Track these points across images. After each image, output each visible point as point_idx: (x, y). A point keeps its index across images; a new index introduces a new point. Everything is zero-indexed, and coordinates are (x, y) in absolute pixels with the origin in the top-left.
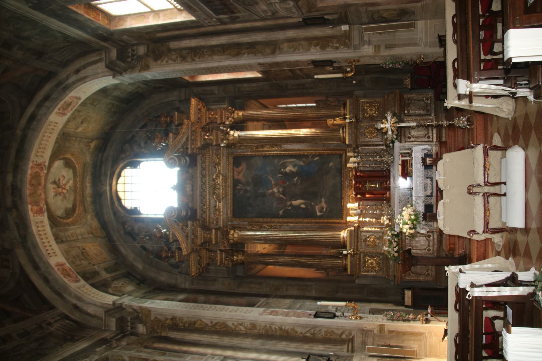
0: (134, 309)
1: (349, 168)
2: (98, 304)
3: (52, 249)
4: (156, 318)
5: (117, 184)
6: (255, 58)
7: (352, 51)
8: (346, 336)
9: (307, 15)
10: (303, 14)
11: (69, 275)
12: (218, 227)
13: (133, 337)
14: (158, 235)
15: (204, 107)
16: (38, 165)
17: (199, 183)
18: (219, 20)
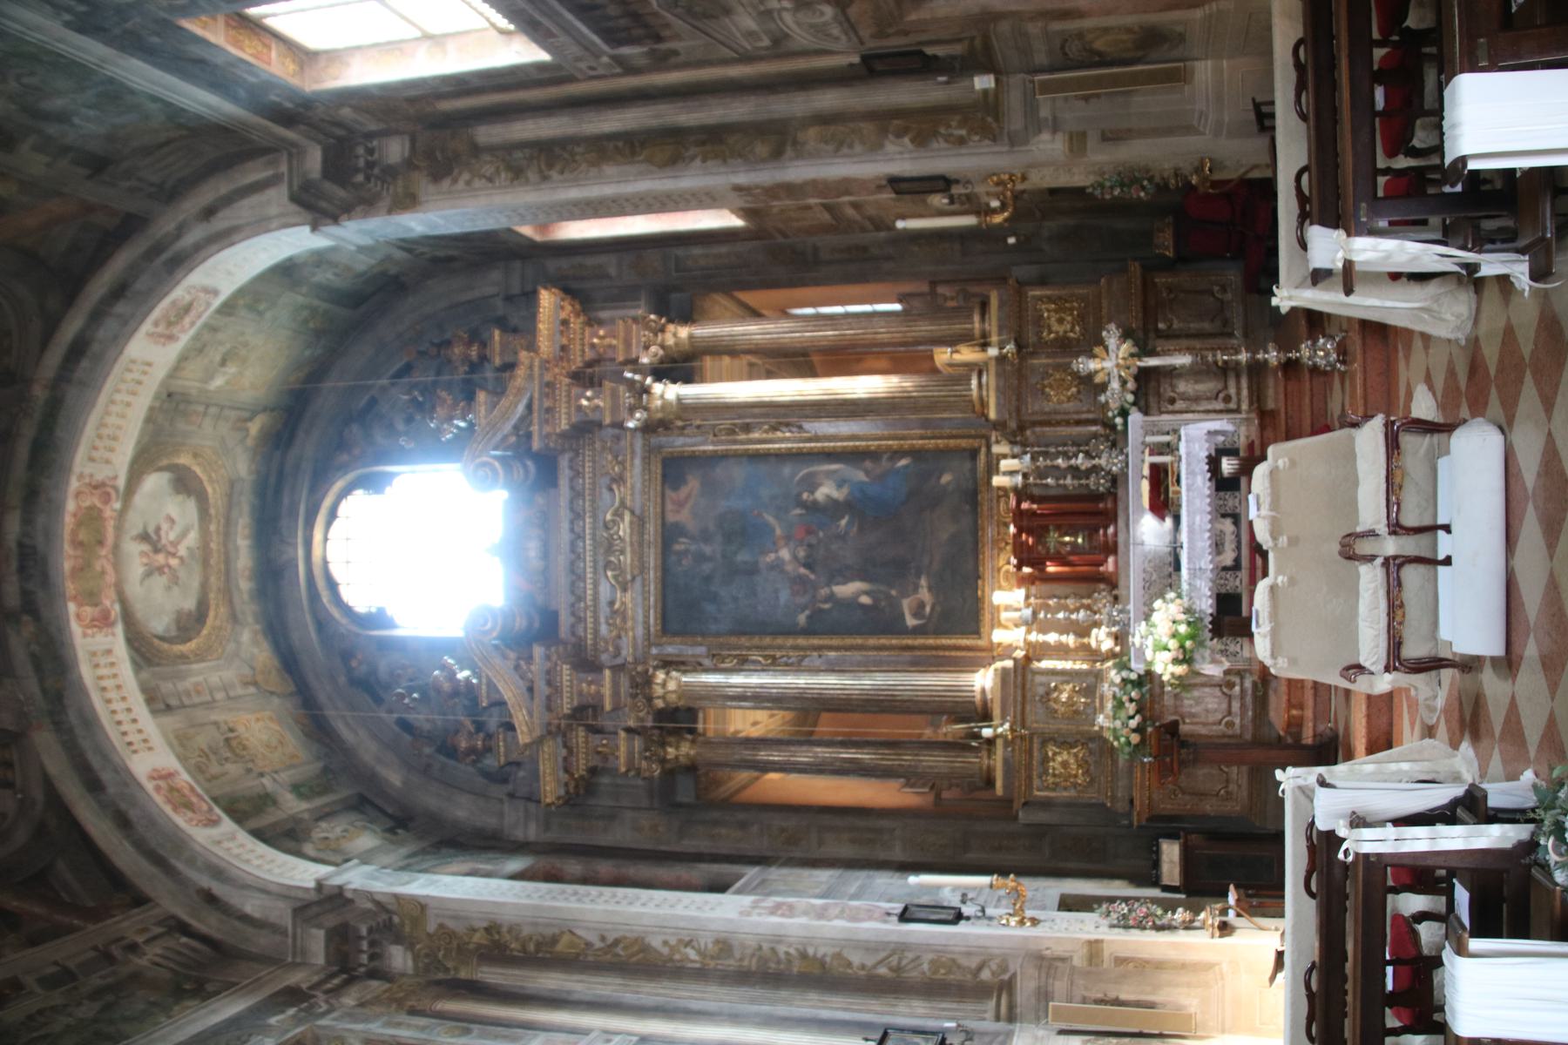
0: (378, 903)
1: (999, 488)
2: (272, 888)
3: (140, 731)
4: (441, 926)
5: (326, 539)
6: (722, 169)
7: (1006, 149)
8: (993, 973)
9: (872, 45)
10: (862, 43)
11: (189, 806)
12: (619, 661)
13: (375, 984)
14: (446, 686)
15: (577, 315)
16: (96, 487)
17: (565, 536)
18: (618, 60)
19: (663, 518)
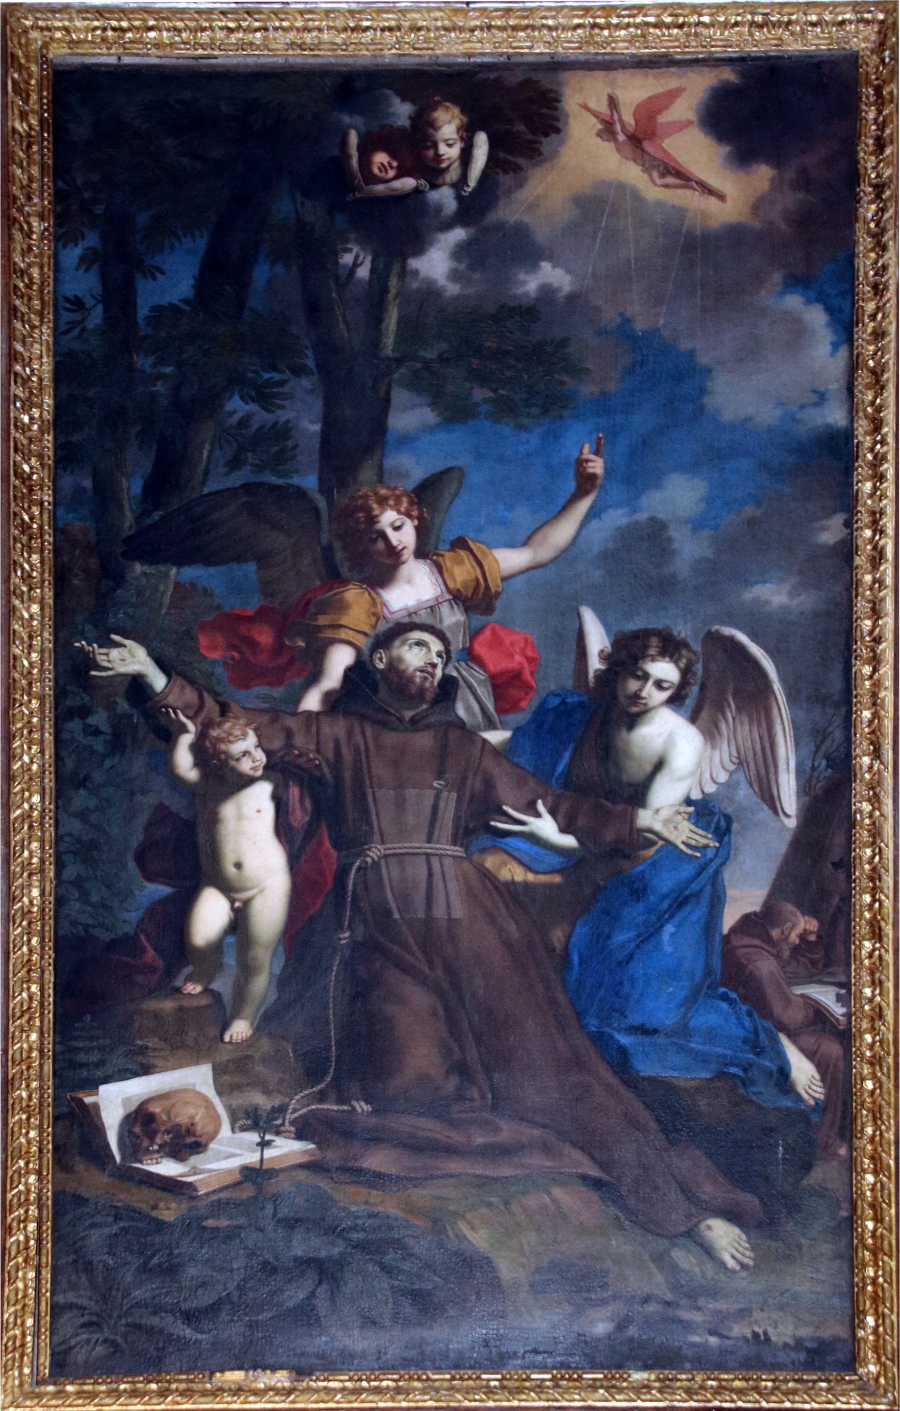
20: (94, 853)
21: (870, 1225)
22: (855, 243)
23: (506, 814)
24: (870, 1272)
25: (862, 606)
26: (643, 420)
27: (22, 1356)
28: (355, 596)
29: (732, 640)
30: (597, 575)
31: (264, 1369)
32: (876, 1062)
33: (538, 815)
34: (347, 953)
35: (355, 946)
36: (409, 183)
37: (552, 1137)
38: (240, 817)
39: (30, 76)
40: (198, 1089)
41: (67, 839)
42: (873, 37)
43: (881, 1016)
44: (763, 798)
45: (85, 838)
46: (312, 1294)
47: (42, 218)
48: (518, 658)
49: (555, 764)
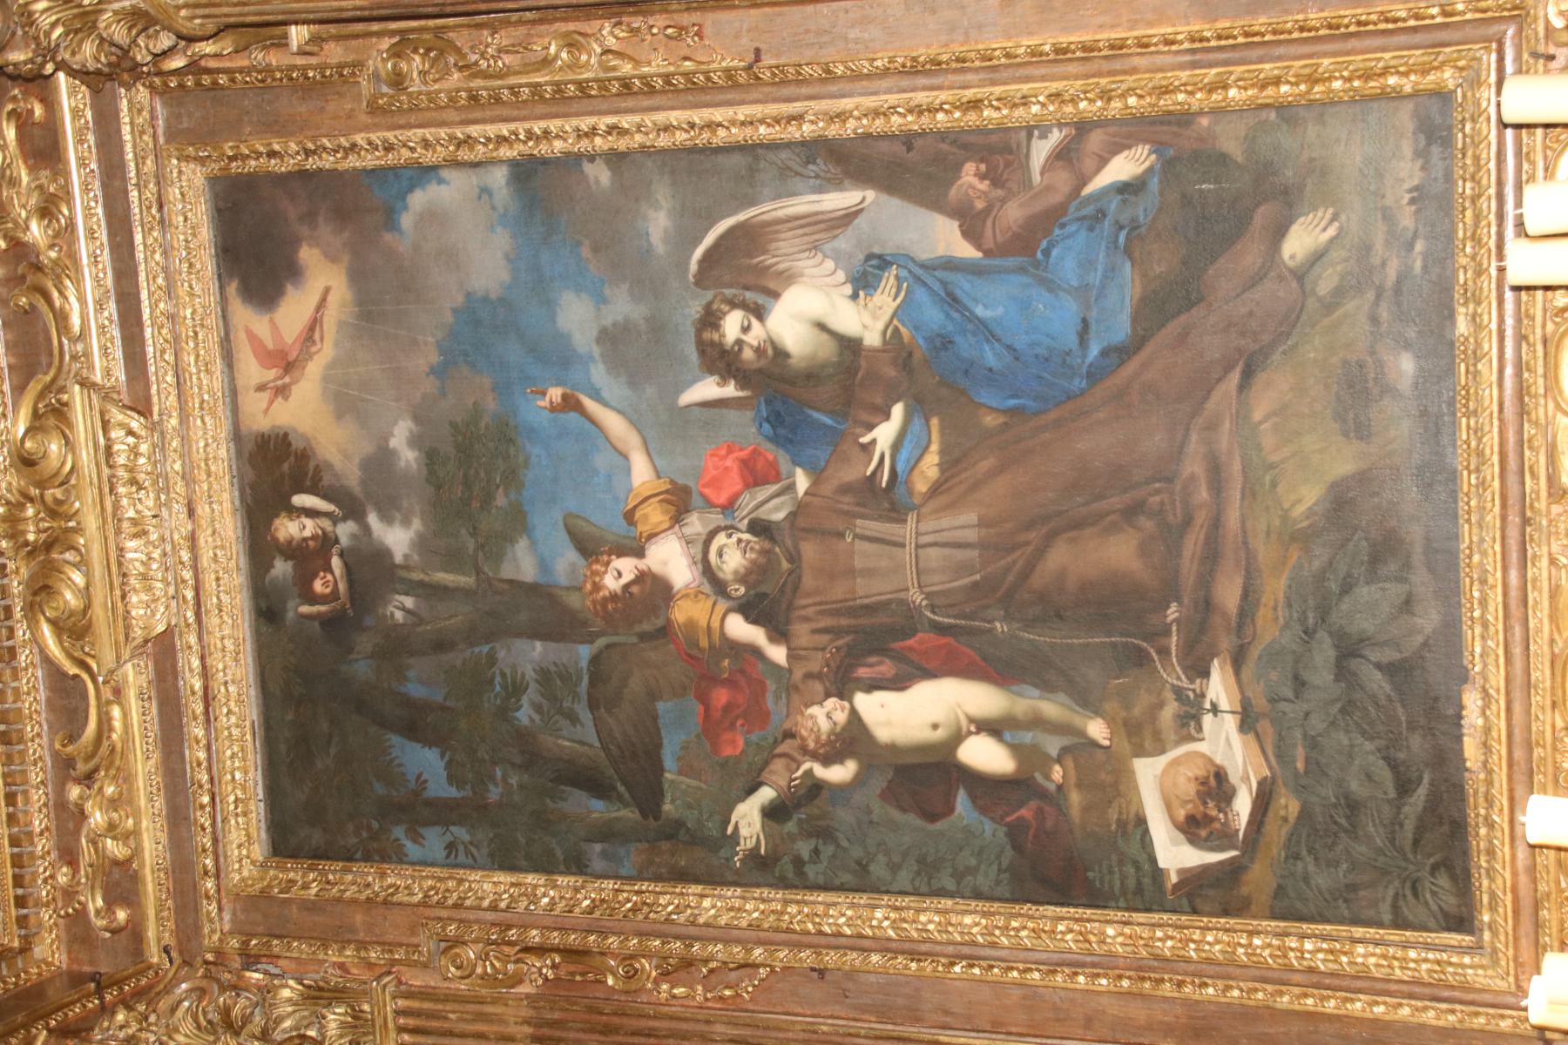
19: (235, 410)
20: (929, 860)
21: (1284, 89)
22: (354, 169)
23: (874, 473)
24: (1337, 85)
25: (663, 141)
26: (512, 352)
27: (1450, 964)
28: (681, 613)
29: (701, 262)
30: (650, 391)
31: (1460, 717)
32: (1106, 95)
33: (874, 441)
34: (1016, 625)
35: (1008, 618)
36: (336, 562)
37: (1200, 421)
38: (889, 723)
39: (276, 877)
40: (1159, 772)
41: (917, 884)
42: (192, 166)
43: (1058, 95)
44: (847, 225)
45: (916, 868)
46: (1378, 666)
47: (383, 875)
48: (729, 463)
49: (826, 426)
